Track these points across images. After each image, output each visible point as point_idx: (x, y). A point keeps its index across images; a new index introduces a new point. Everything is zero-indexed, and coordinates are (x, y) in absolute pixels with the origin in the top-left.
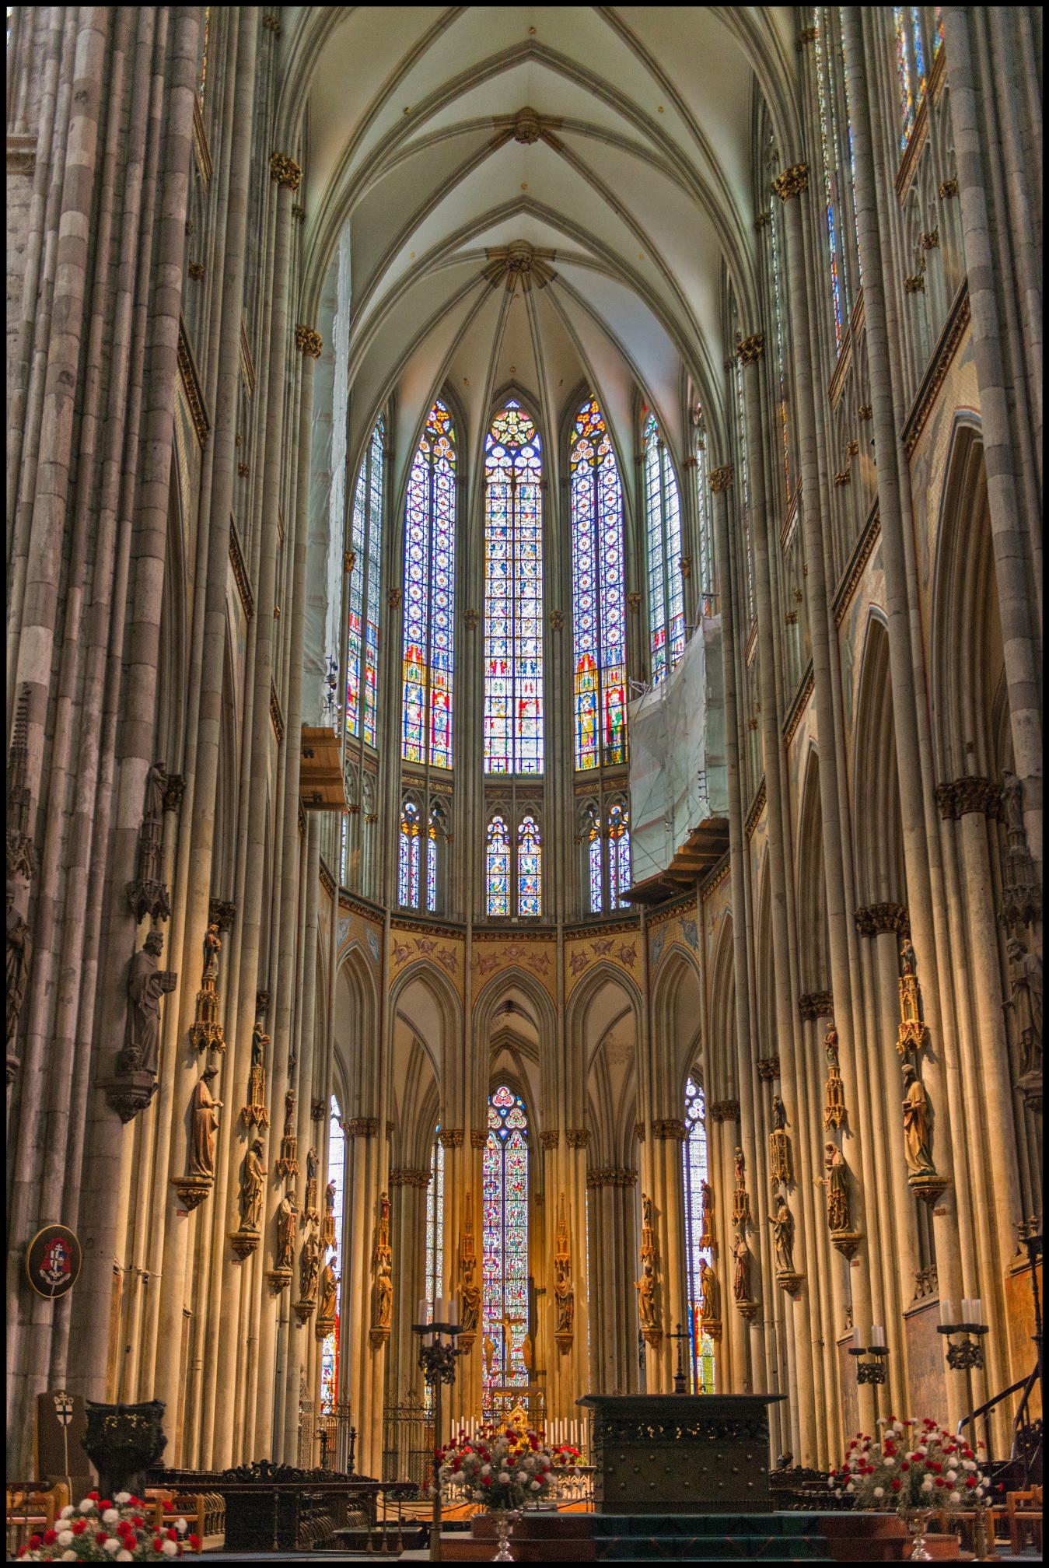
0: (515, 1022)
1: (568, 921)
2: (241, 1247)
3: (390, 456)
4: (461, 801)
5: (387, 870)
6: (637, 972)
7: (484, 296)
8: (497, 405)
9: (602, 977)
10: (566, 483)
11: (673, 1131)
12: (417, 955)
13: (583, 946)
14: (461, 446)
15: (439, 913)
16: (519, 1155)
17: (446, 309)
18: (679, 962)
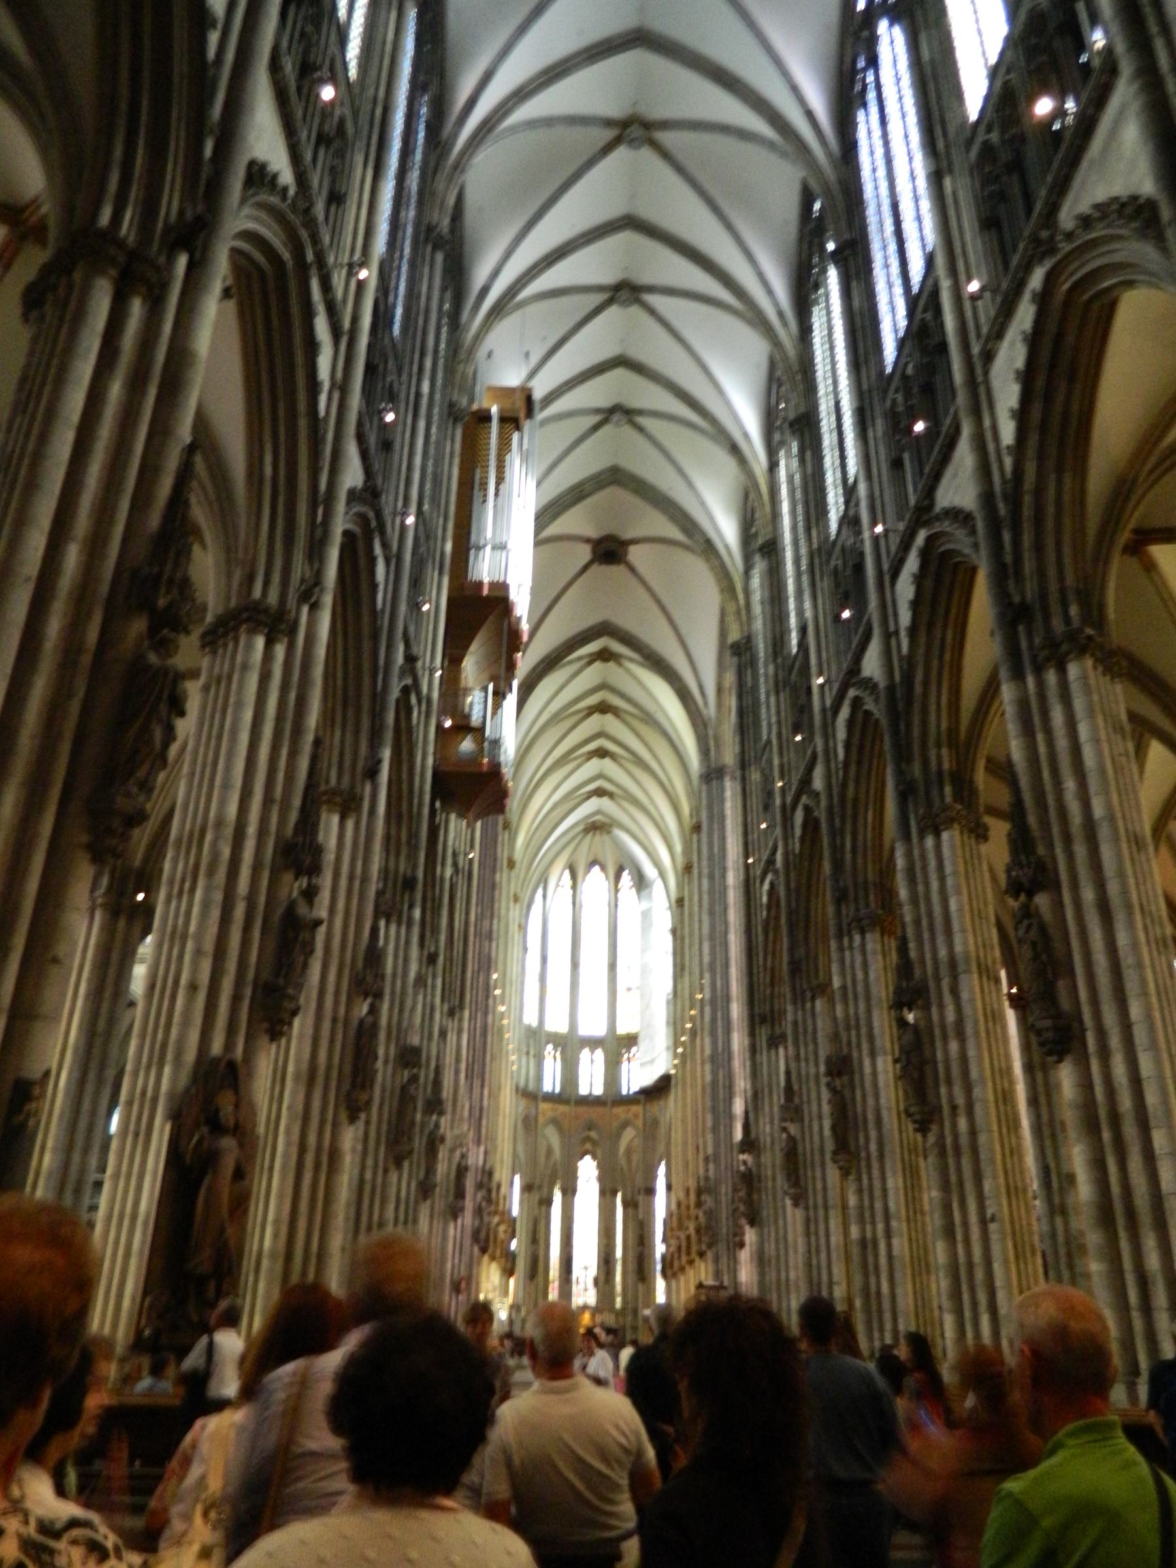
0: (593, 1134)
1: (613, 1099)
2: (493, 1258)
3: (545, 896)
4: (570, 1046)
5: (539, 1078)
6: (640, 1122)
7: (584, 837)
8: (589, 871)
9: (625, 1125)
10: (616, 905)
11: (650, 1191)
12: (550, 1114)
13: (619, 1110)
14: (574, 887)
15: (560, 1094)
16: (595, 1188)
17: (568, 843)
18: (655, 1123)
